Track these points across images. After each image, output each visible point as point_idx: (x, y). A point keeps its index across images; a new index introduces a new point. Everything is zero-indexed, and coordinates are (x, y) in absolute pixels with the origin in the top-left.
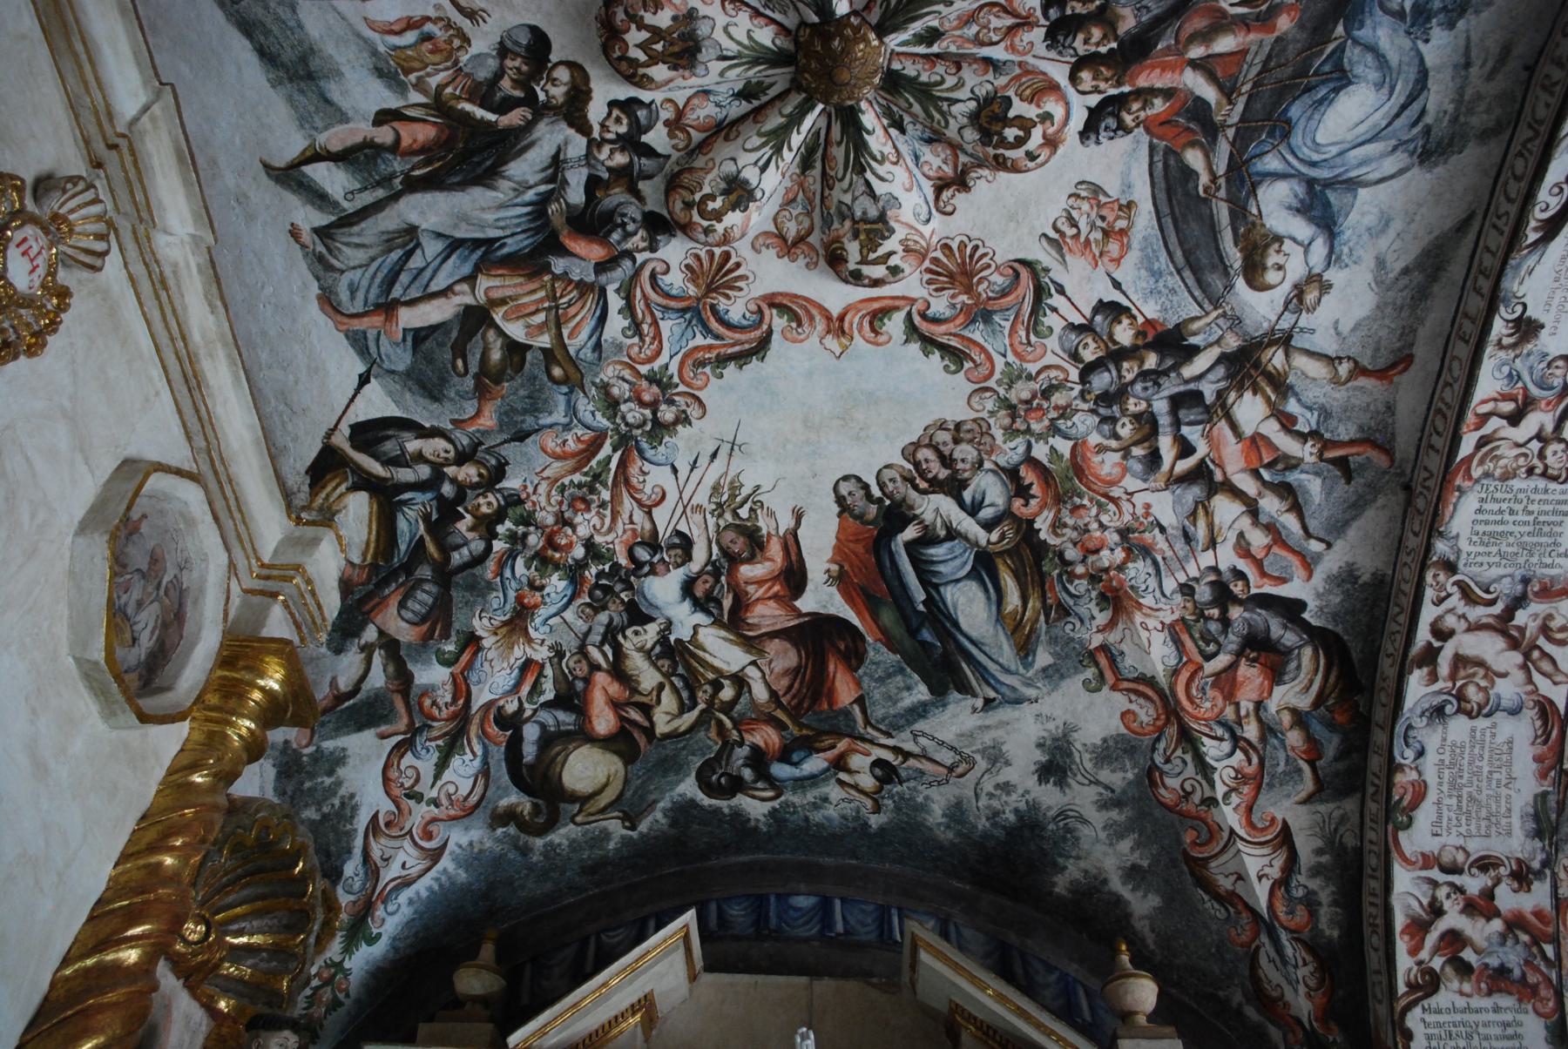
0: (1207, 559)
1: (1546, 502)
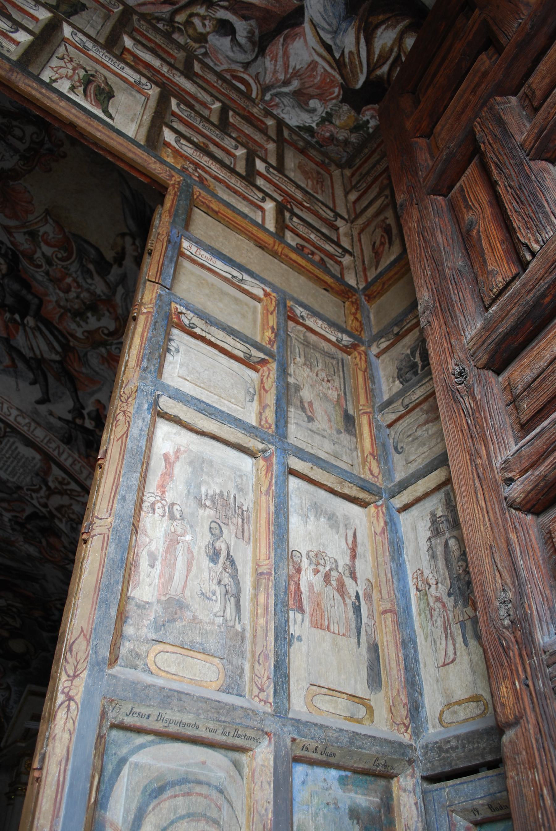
0: (6, 519)
1: (7, 452)
